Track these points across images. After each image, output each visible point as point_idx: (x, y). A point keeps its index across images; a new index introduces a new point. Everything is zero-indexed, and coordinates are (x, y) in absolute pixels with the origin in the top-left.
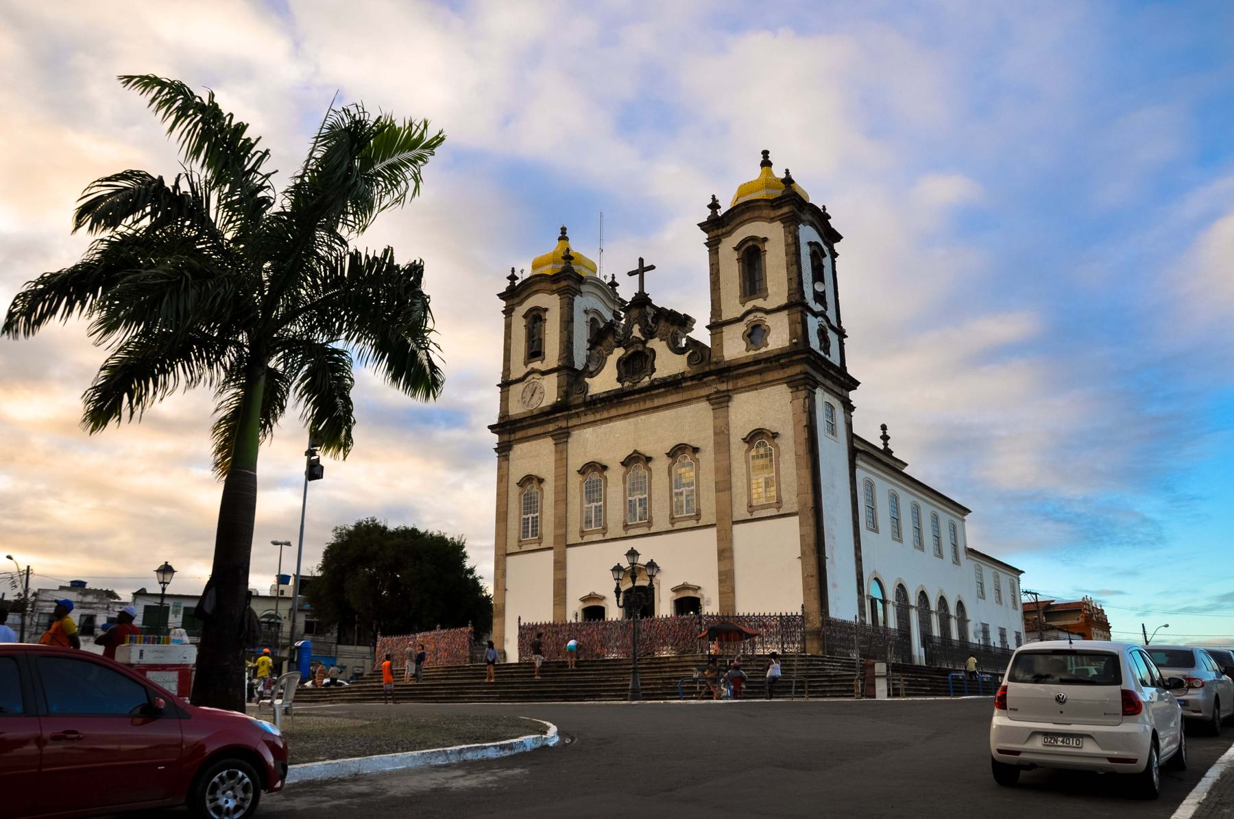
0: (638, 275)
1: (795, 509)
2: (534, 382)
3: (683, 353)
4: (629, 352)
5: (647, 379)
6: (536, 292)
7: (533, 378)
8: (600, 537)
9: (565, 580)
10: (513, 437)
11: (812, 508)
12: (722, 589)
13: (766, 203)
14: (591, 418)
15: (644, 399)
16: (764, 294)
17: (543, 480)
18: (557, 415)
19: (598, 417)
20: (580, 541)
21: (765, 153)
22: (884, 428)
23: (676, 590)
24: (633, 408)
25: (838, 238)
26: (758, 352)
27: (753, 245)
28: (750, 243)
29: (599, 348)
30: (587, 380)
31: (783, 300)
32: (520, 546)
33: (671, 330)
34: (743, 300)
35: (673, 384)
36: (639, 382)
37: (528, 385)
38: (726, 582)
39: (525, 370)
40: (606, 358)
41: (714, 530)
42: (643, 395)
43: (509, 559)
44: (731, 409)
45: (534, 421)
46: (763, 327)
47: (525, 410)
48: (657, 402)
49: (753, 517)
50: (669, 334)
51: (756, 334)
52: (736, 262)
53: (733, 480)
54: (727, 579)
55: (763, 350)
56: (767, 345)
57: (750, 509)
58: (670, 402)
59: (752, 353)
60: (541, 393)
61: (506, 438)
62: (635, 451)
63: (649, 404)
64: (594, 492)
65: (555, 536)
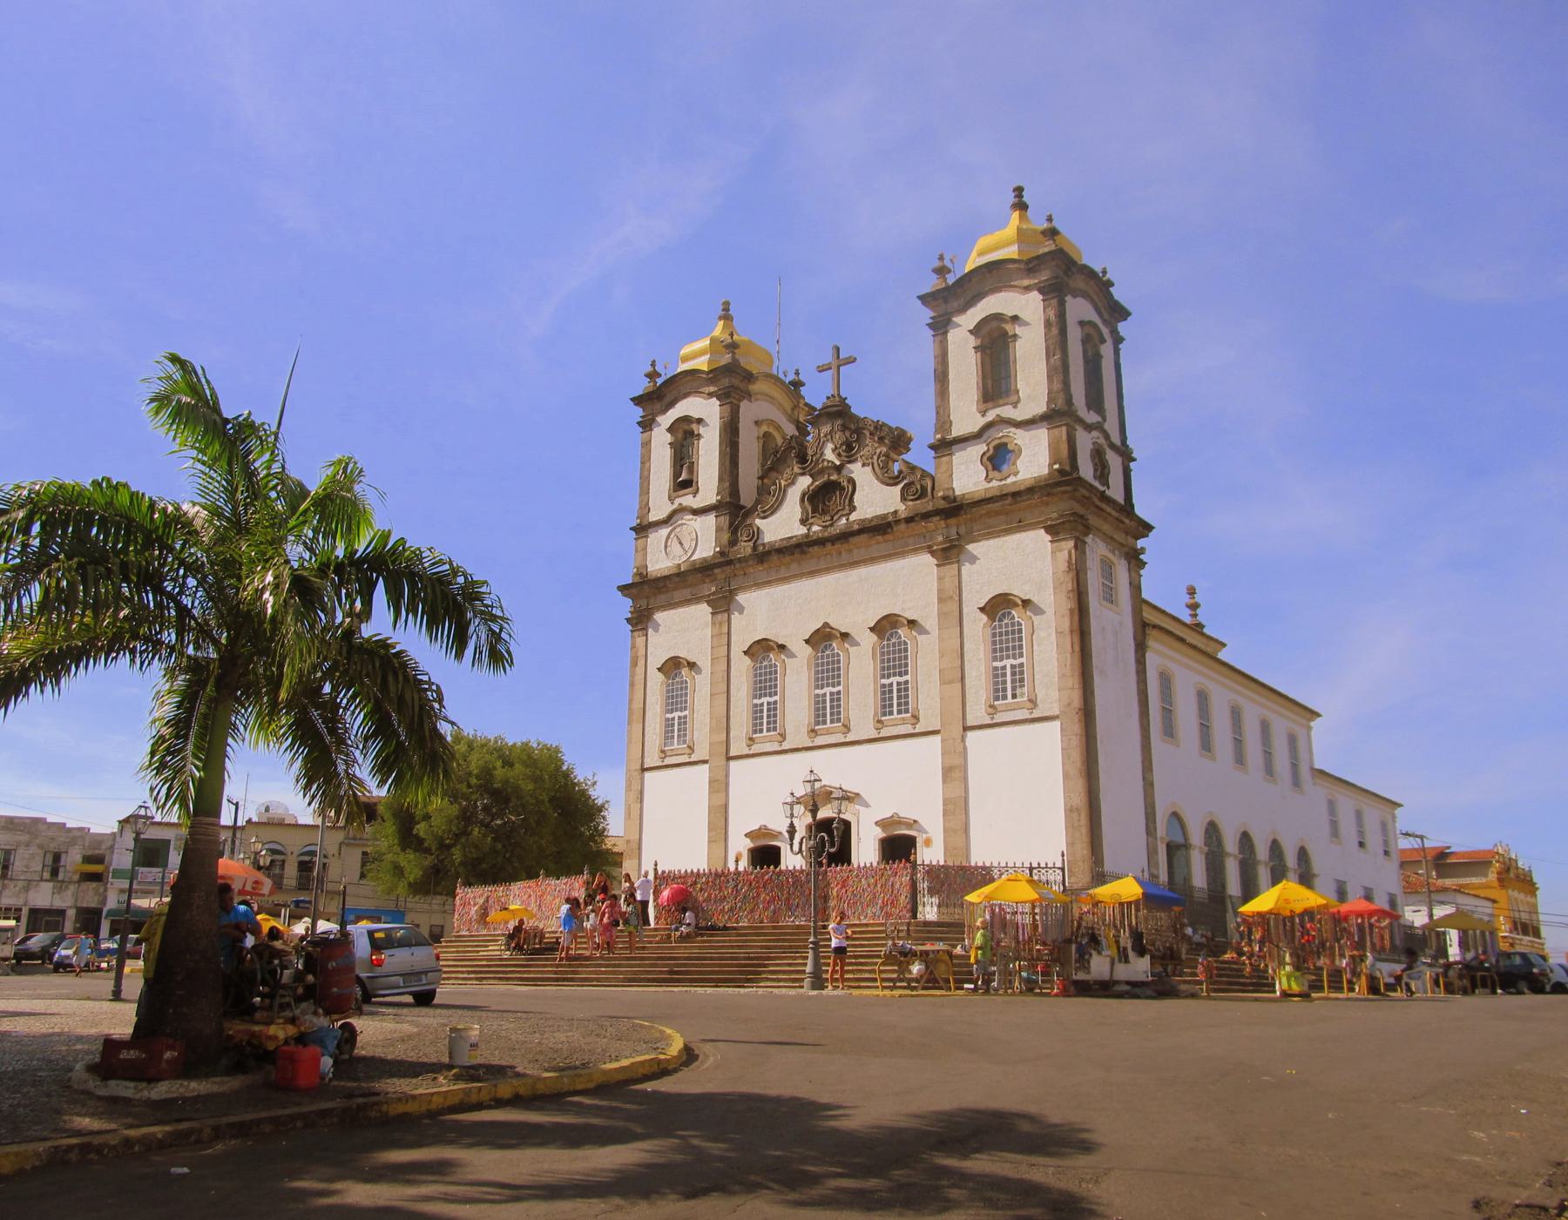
0: (831, 372)
3: (896, 484)
5: (844, 521)
6: (686, 396)
8: (776, 747)
11: (1080, 709)
16: (1013, 398)
17: (695, 663)
20: (746, 751)
21: (1019, 191)
22: (1192, 591)
23: (881, 824)
25: (1122, 313)
28: (994, 324)
30: (758, 522)
31: (1040, 407)
33: (878, 451)
34: (983, 407)
35: (880, 528)
39: (668, 508)
41: (938, 738)
46: (1010, 447)
50: (875, 457)
51: (998, 458)
52: (973, 350)
54: (957, 810)
59: (995, 483)
61: (643, 603)
62: (826, 625)
64: (765, 684)
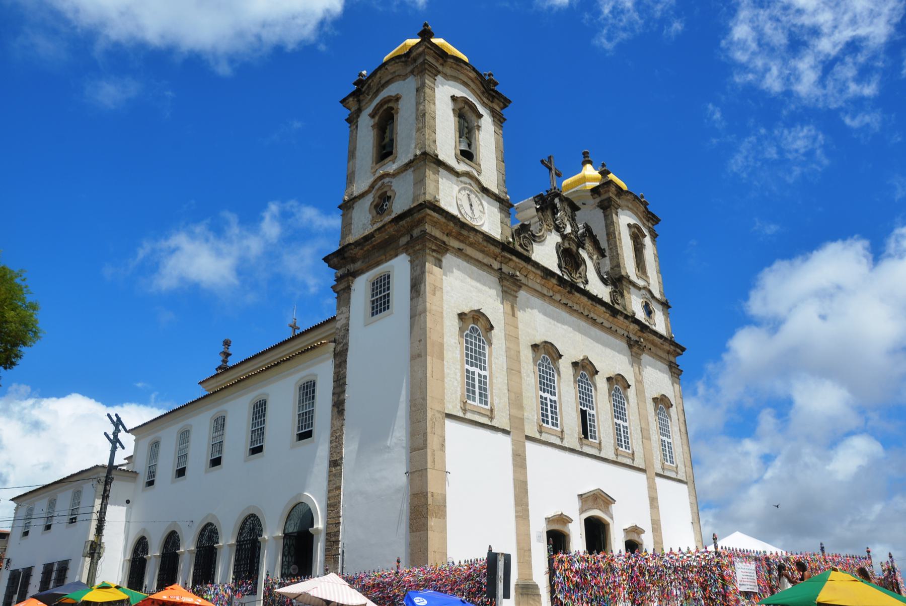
7: (470, 185)
18: (514, 258)
45: (485, 244)
65: (511, 417)
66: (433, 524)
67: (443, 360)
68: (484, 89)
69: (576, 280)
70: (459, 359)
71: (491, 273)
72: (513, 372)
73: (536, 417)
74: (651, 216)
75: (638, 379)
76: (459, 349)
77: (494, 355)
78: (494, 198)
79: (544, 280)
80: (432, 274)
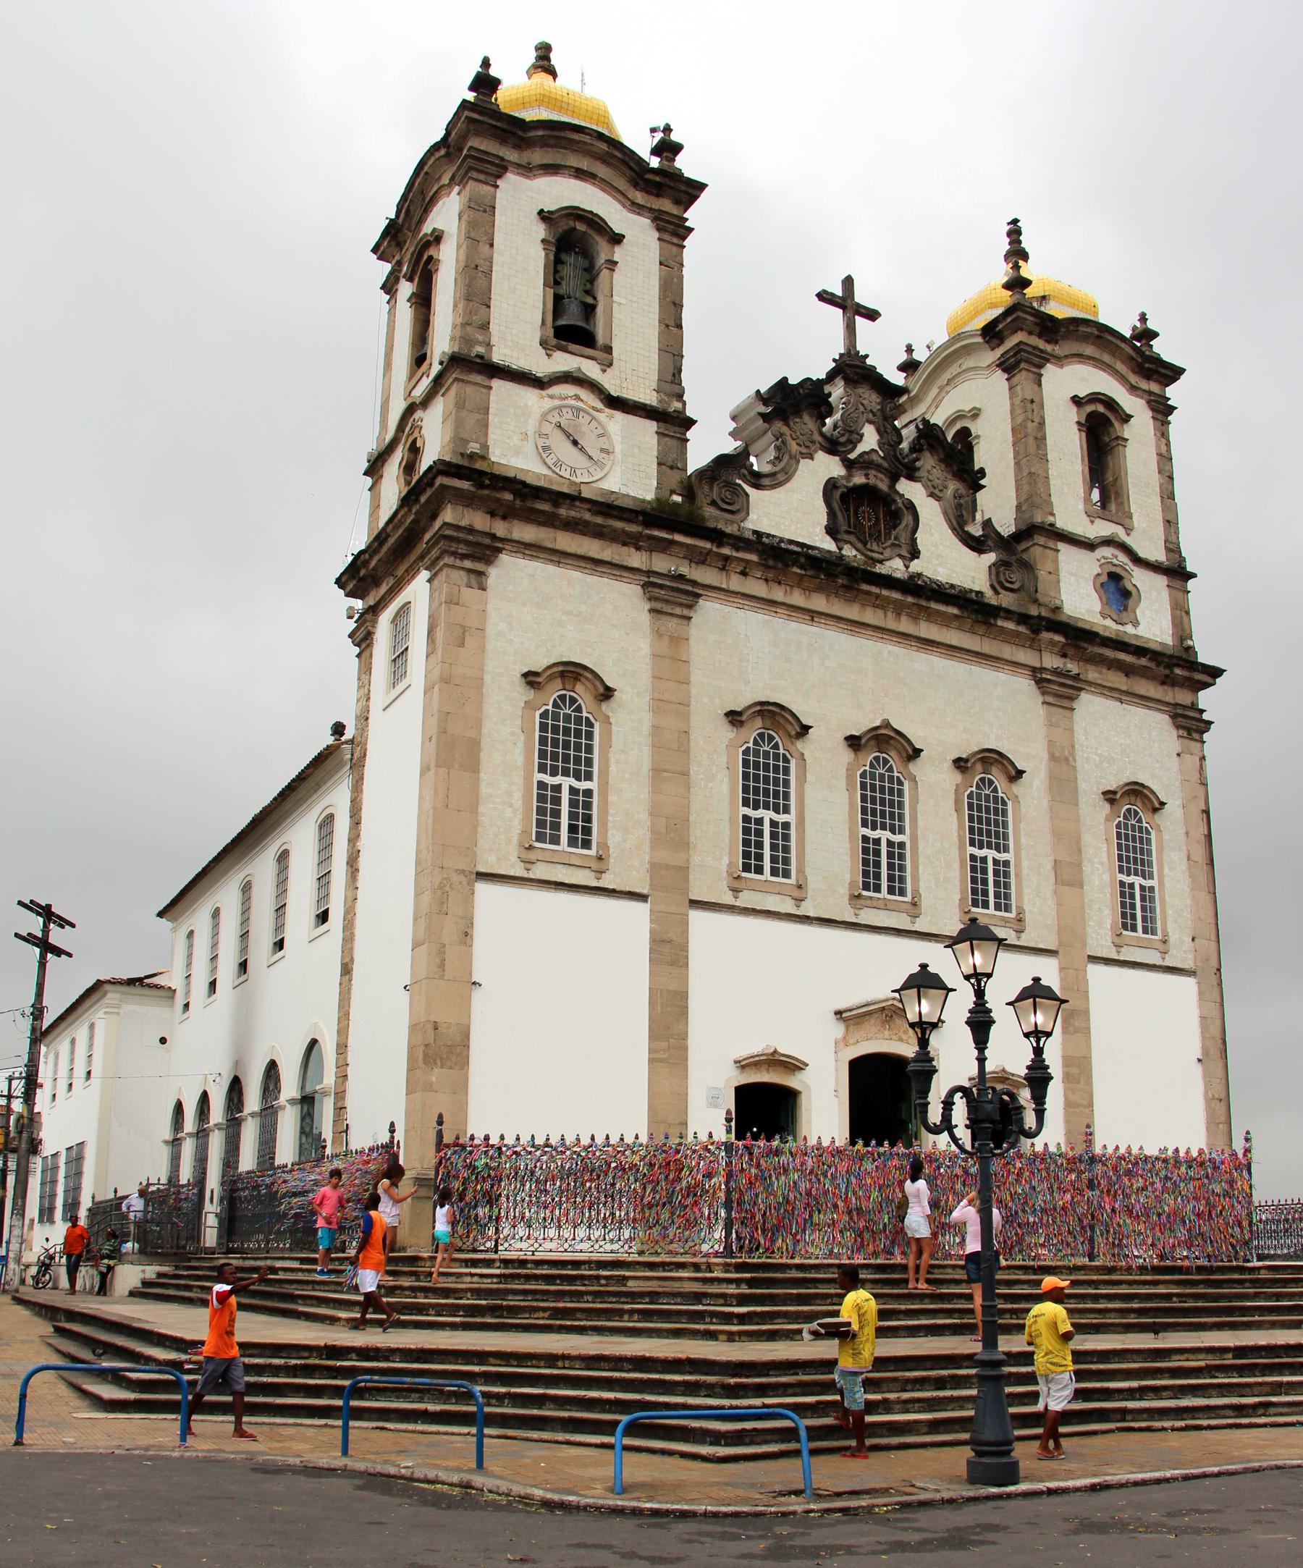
1: (1188, 964)
2: (579, 410)
4: (859, 479)
7: (577, 398)
8: (787, 906)
9: (684, 995)
10: (500, 528)
12: (1072, 1097)
13: (1133, 354)
14: (756, 587)
15: (899, 609)
18: (679, 538)
19: (778, 594)
20: (728, 899)
24: (870, 616)
26: (1120, 628)
27: (1103, 415)
28: (1101, 409)
29: (778, 426)
32: (528, 863)
36: (881, 562)
37: (560, 408)
38: (1078, 1082)
40: (798, 462)
42: (910, 599)
43: (482, 888)
44: (1076, 714)
45: (599, 520)
47: (549, 473)
48: (927, 630)
49: (1122, 958)
52: (1076, 428)
53: (1086, 868)
55: (1129, 629)
56: (1136, 623)
57: (1118, 941)
58: (954, 642)
60: (602, 450)
62: (887, 724)
63: (905, 625)
65: (655, 868)
66: (434, 1079)
67: (476, 770)
68: (633, 174)
69: (882, 554)
70: (519, 764)
71: (621, 576)
72: (665, 774)
73: (725, 861)
74: (1153, 366)
75: (1057, 754)
76: (521, 744)
77: (617, 742)
78: (643, 413)
79: (772, 571)
80: (458, 604)
